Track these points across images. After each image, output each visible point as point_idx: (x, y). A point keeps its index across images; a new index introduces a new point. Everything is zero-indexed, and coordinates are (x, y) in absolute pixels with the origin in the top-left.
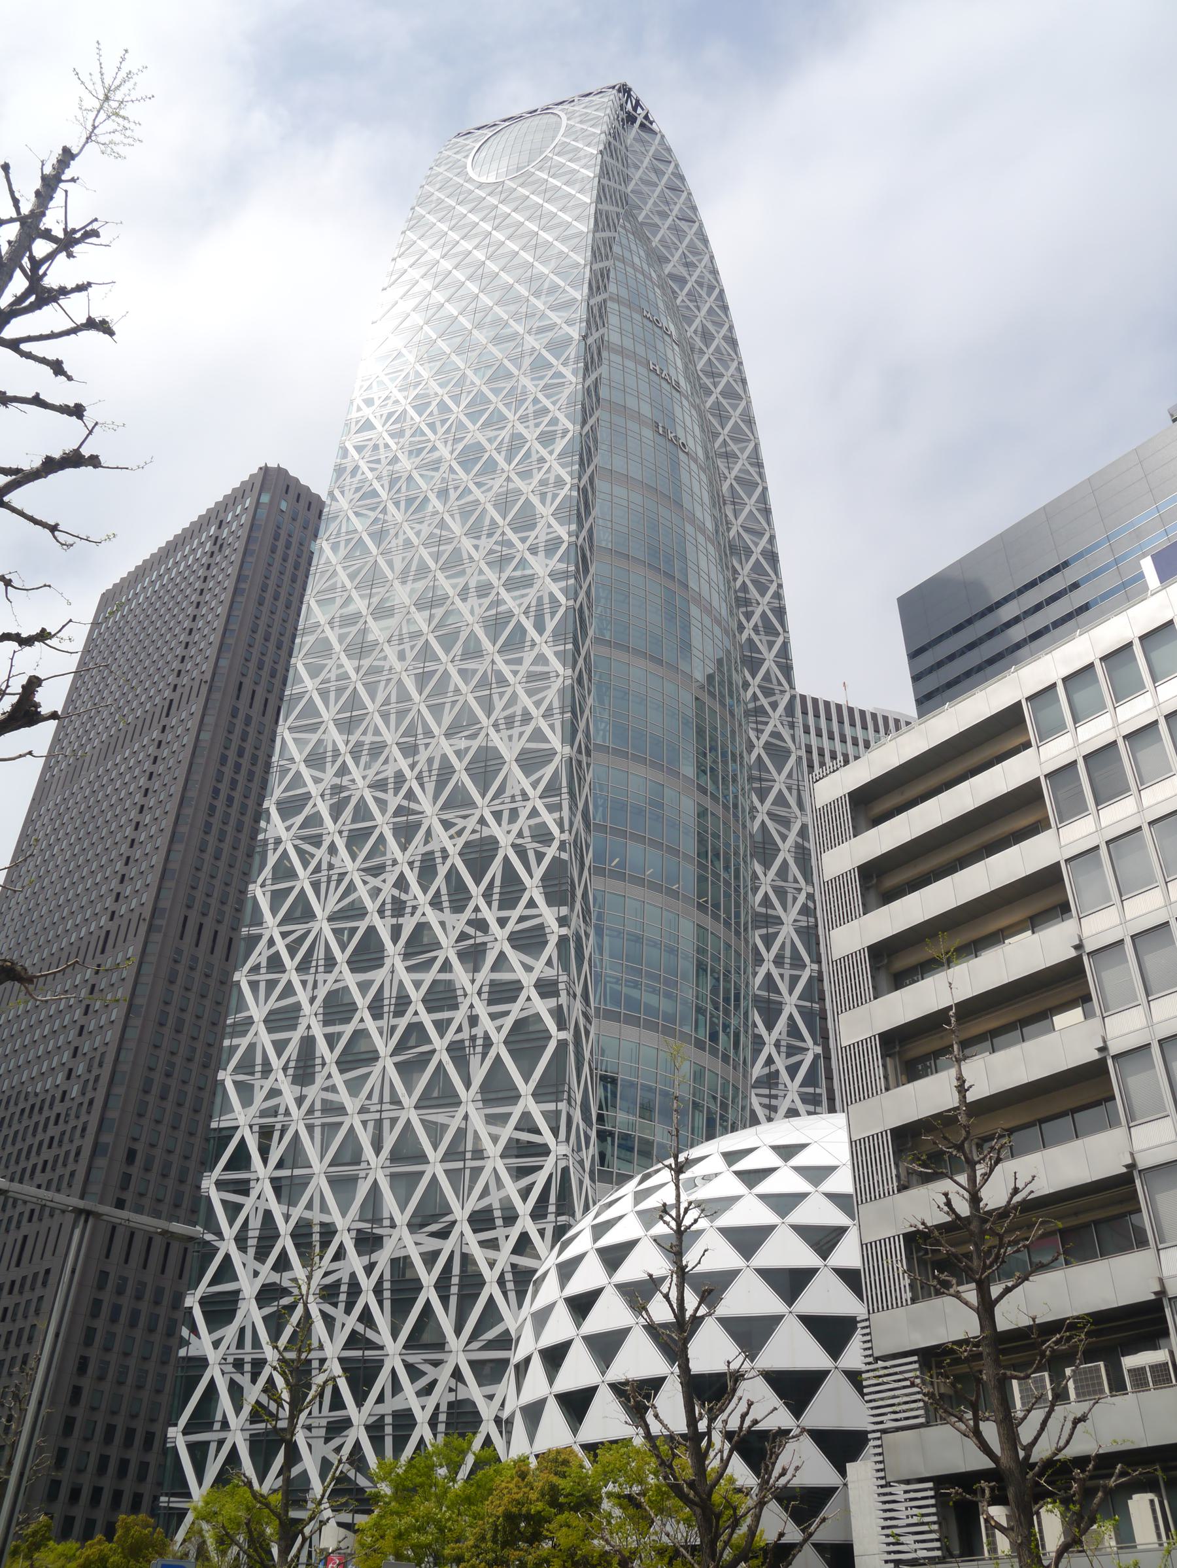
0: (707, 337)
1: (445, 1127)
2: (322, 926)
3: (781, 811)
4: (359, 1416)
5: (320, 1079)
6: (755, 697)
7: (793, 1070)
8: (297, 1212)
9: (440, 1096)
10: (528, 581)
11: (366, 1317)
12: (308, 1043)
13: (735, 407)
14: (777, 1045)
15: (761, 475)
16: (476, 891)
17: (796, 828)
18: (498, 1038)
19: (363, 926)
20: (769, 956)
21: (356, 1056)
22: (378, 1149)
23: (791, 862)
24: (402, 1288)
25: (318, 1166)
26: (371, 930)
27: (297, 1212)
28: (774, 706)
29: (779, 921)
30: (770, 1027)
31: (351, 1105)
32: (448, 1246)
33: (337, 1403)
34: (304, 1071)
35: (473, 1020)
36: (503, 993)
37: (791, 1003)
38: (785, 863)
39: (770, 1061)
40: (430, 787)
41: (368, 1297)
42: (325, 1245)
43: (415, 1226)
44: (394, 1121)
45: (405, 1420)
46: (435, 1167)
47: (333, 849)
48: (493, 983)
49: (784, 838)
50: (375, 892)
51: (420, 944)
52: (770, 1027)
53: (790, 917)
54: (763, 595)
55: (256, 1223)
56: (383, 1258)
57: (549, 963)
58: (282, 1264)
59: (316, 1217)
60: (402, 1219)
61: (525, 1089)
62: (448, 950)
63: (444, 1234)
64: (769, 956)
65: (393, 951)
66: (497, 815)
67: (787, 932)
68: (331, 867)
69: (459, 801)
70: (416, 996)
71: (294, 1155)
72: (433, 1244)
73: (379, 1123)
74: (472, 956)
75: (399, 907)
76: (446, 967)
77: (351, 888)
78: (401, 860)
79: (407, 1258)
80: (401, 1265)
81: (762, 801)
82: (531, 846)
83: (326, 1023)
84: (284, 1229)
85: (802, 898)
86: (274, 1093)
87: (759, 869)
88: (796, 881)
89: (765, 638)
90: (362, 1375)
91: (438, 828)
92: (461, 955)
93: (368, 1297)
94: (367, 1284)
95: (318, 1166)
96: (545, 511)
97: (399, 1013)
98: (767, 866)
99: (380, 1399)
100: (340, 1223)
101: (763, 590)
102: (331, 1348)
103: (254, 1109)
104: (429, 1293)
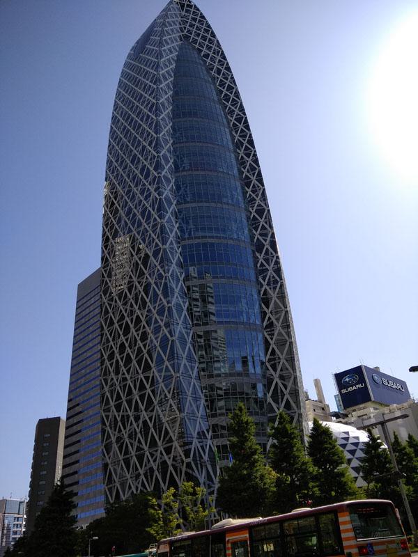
0: (219, 71)
1: (149, 377)
2: (116, 325)
3: (264, 232)
4: (141, 472)
5: (121, 372)
6: (250, 195)
7: (278, 320)
8: (121, 414)
9: (147, 368)
10: (149, 195)
11: (139, 442)
12: (117, 361)
13: (231, 93)
14: (271, 313)
15: (245, 114)
16: (147, 300)
17: (269, 236)
18: (157, 345)
19: (125, 322)
20: (265, 283)
21: (129, 360)
22: (135, 389)
23: (269, 248)
26: (127, 322)
27: (121, 414)
28: (257, 196)
29: (267, 270)
30: (268, 308)
31: (128, 377)
32: (154, 413)
33: (137, 469)
35: (152, 341)
38: (267, 248)
39: (269, 318)
40: (134, 272)
41: (139, 435)
42: (128, 421)
43: (146, 410)
44: (138, 379)
45: (151, 469)
46: (149, 391)
47: (116, 301)
48: (155, 328)
49: (266, 240)
50: (126, 310)
52: (268, 308)
53: (270, 268)
54: (249, 157)
55: (113, 420)
56: (141, 422)
57: (166, 317)
58: (120, 431)
59: (125, 414)
60: (143, 408)
61: (165, 359)
63: (152, 411)
64: (265, 283)
66: (150, 275)
67: (271, 272)
68: (116, 306)
70: (138, 338)
71: (119, 397)
72: (150, 414)
73: (135, 380)
74: (149, 323)
75: (132, 313)
76: (144, 327)
77: (121, 311)
79: (146, 420)
80: (145, 422)
81: (256, 231)
82: (159, 281)
83: (120, 355)
84: (119, 419)
85: (275, 258)
86: (112, 379)
87: (258, 255)
88: (272, 254)
89: (251, 173)
90: (140, 458)
91: (137, 284)
92: (147, 322)
93: (139, 435)
94: (138, 431)
97: (135, 346)
98: (261, 253)
99: (146, 466)
100: (130, 413)
101: (248, 155)
102: (133, 452)
103: (108, 386)
104: (152, 430)
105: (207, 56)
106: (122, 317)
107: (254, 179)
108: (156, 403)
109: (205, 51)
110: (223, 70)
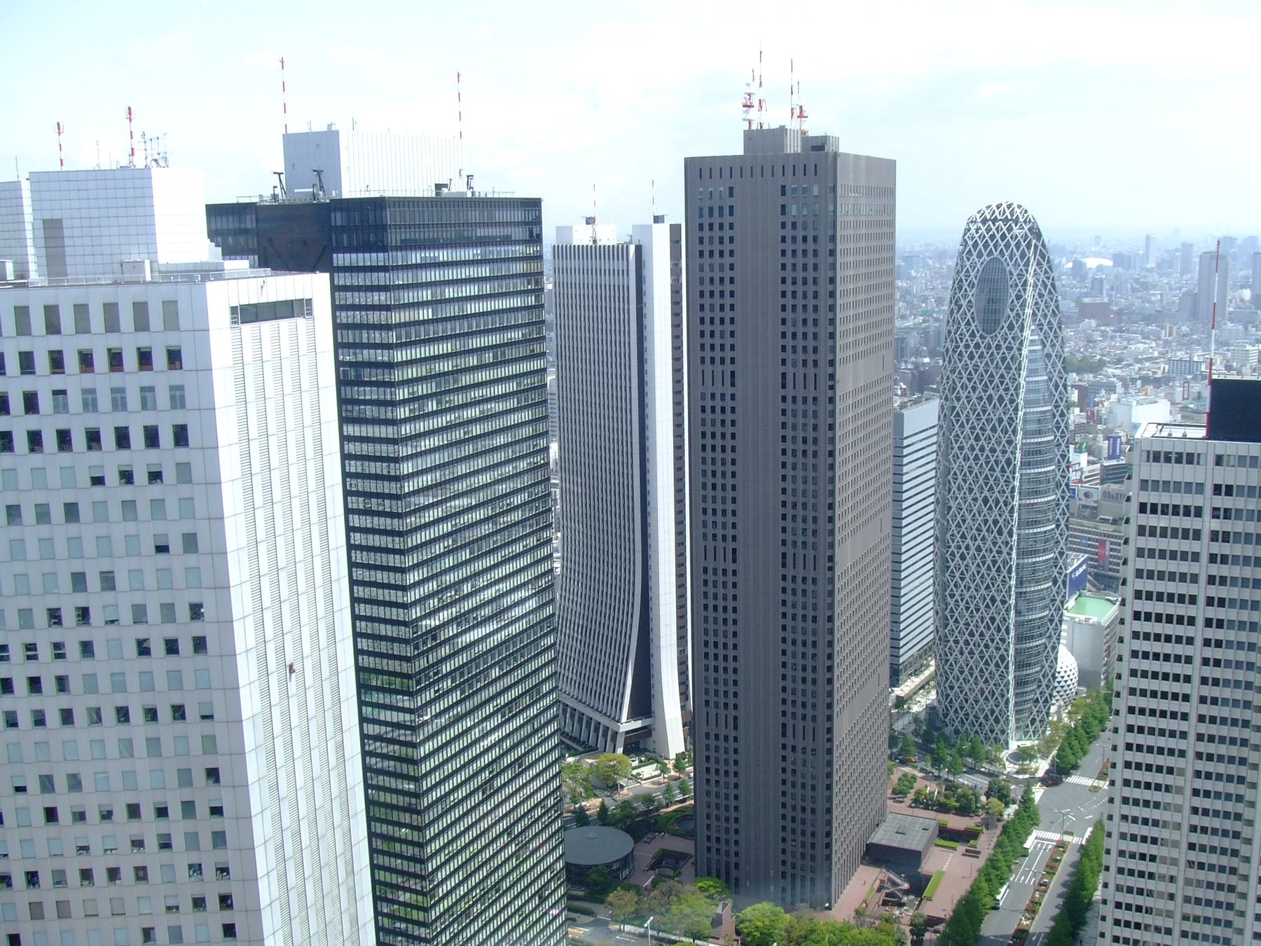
0: (1057, 387)
2: (961, 625)
9: (987, 663)
21: (971, 653)
24: (982, 692)
25: (966, 671)
34: (962, 653)
36: (998, 649)
37: (1056, 620)
51: (982, 635)
62: (987, 638)
65: (977, 635)
67: (1058, 602)
69: (987, 606)
78: (977, 616)
95: (966, 671)
96: (1005, 531)
105: (1048, 356)
106: (968, 624)
107: (1063, 523)
108: (992, 683)
109: (1048, 349)
110: (1061, 387)
